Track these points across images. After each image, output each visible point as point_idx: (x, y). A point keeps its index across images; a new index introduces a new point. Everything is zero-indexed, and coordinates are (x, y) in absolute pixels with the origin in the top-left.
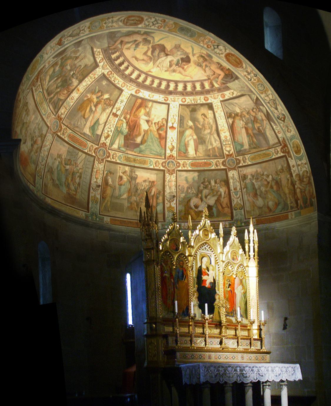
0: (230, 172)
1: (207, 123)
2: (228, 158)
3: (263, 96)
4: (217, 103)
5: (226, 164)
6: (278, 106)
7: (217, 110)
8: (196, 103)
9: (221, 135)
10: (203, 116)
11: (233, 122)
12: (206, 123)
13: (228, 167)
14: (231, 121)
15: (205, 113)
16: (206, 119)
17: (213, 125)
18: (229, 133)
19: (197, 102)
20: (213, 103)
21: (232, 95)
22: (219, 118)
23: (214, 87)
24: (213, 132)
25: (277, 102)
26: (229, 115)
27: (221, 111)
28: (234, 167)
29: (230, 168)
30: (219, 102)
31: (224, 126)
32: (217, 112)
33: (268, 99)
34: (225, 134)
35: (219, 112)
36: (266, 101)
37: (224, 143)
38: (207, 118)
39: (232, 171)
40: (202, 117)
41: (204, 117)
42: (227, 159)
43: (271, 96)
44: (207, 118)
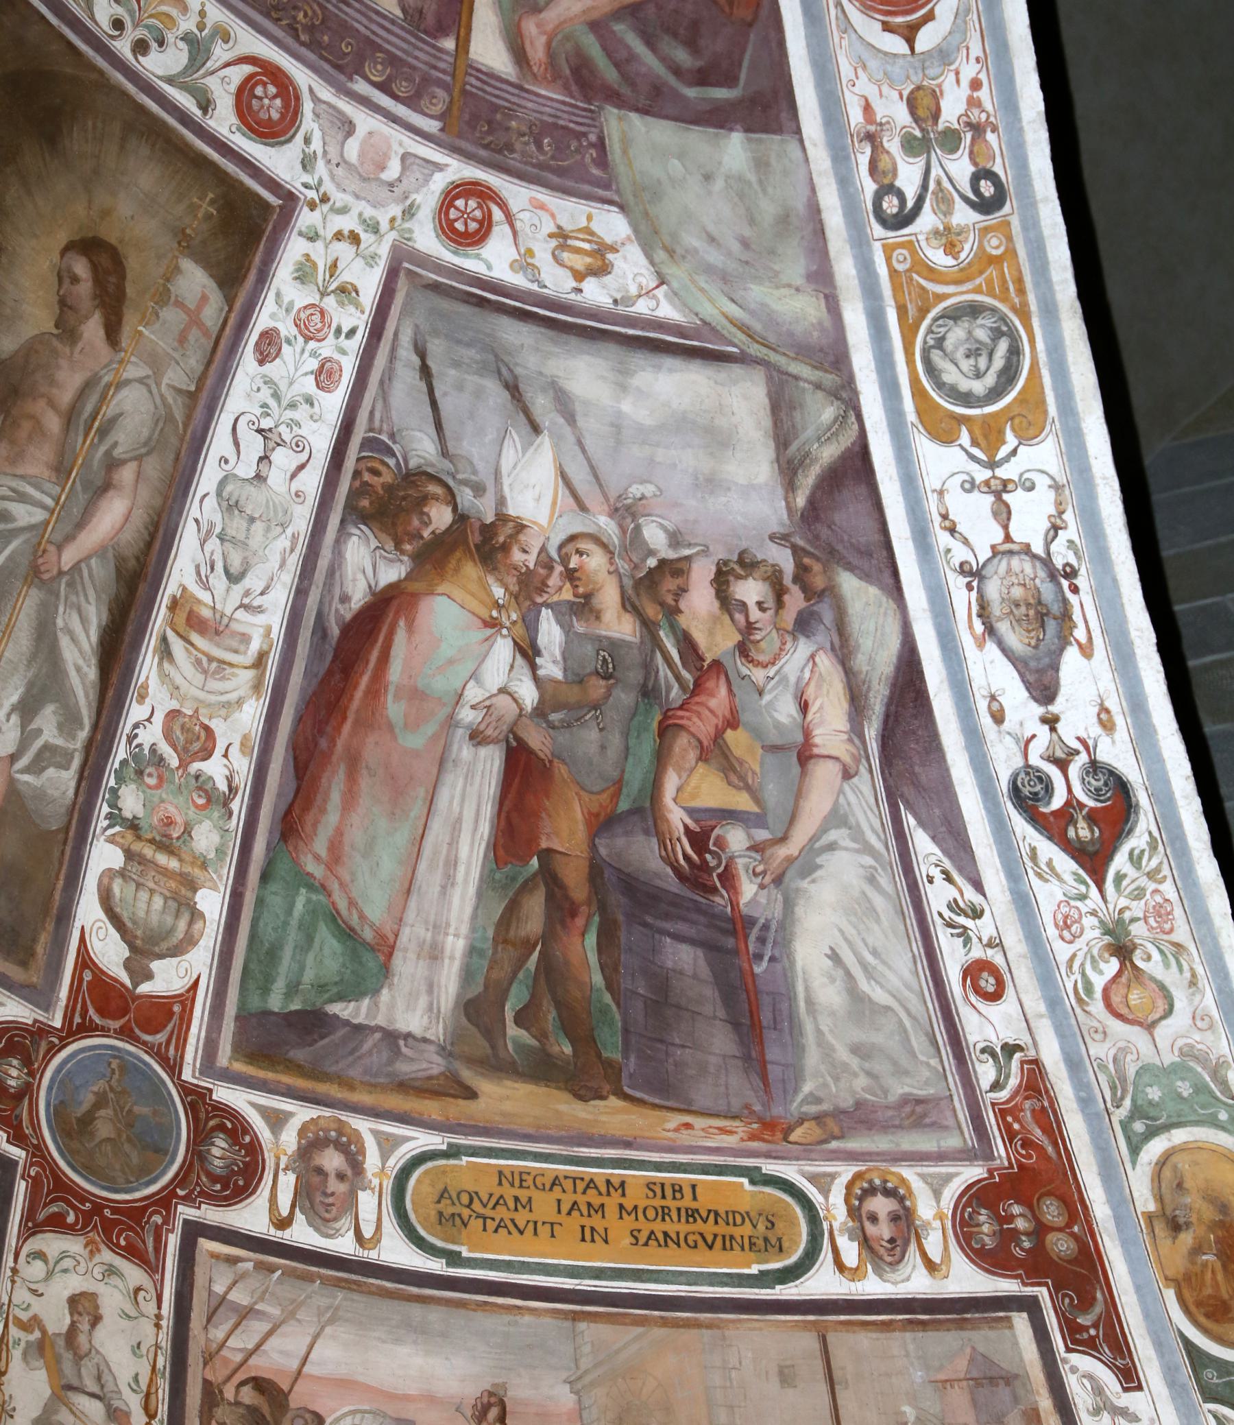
0: (52, 1243)
1: (66, 398)
2: (87, 1029)
3: (942, 463)
4: (344, 250)
5: (27, 1091)
6: (1071, 658)
7: (286, 328)
8: (123, 47)
9: (148, 667)
10: (81, 267)
11: (385, 608)
12: (69, 382)
13: (38, 1152)
14: (366, 565)
15: (133, 264)
16: (93, 329)
17: (126, 474)
18: (252, 715)
19: (141, 47)
20: (306, 218)
21: (579, 276)
22: (253, 446)
23: (449, 44)
24: (69, 557)
25: (1084, 605)
26: (377, 491)
27: (325, 375)
28: (135, 1214)
29: (62, 1188)
30: (371, 260)
31: (254, 581)
32: (269, 347)
33: (984, 534)
34: (211, 699)
35: (295, 366)
36: (944, 539)
37: (131, 802)
38: (112, 333)
39: (74, 1245)
40: (64, 277)
41: (85, 288)
42: (72, 1031)
43: (1030, 517)
44: (112, 333)
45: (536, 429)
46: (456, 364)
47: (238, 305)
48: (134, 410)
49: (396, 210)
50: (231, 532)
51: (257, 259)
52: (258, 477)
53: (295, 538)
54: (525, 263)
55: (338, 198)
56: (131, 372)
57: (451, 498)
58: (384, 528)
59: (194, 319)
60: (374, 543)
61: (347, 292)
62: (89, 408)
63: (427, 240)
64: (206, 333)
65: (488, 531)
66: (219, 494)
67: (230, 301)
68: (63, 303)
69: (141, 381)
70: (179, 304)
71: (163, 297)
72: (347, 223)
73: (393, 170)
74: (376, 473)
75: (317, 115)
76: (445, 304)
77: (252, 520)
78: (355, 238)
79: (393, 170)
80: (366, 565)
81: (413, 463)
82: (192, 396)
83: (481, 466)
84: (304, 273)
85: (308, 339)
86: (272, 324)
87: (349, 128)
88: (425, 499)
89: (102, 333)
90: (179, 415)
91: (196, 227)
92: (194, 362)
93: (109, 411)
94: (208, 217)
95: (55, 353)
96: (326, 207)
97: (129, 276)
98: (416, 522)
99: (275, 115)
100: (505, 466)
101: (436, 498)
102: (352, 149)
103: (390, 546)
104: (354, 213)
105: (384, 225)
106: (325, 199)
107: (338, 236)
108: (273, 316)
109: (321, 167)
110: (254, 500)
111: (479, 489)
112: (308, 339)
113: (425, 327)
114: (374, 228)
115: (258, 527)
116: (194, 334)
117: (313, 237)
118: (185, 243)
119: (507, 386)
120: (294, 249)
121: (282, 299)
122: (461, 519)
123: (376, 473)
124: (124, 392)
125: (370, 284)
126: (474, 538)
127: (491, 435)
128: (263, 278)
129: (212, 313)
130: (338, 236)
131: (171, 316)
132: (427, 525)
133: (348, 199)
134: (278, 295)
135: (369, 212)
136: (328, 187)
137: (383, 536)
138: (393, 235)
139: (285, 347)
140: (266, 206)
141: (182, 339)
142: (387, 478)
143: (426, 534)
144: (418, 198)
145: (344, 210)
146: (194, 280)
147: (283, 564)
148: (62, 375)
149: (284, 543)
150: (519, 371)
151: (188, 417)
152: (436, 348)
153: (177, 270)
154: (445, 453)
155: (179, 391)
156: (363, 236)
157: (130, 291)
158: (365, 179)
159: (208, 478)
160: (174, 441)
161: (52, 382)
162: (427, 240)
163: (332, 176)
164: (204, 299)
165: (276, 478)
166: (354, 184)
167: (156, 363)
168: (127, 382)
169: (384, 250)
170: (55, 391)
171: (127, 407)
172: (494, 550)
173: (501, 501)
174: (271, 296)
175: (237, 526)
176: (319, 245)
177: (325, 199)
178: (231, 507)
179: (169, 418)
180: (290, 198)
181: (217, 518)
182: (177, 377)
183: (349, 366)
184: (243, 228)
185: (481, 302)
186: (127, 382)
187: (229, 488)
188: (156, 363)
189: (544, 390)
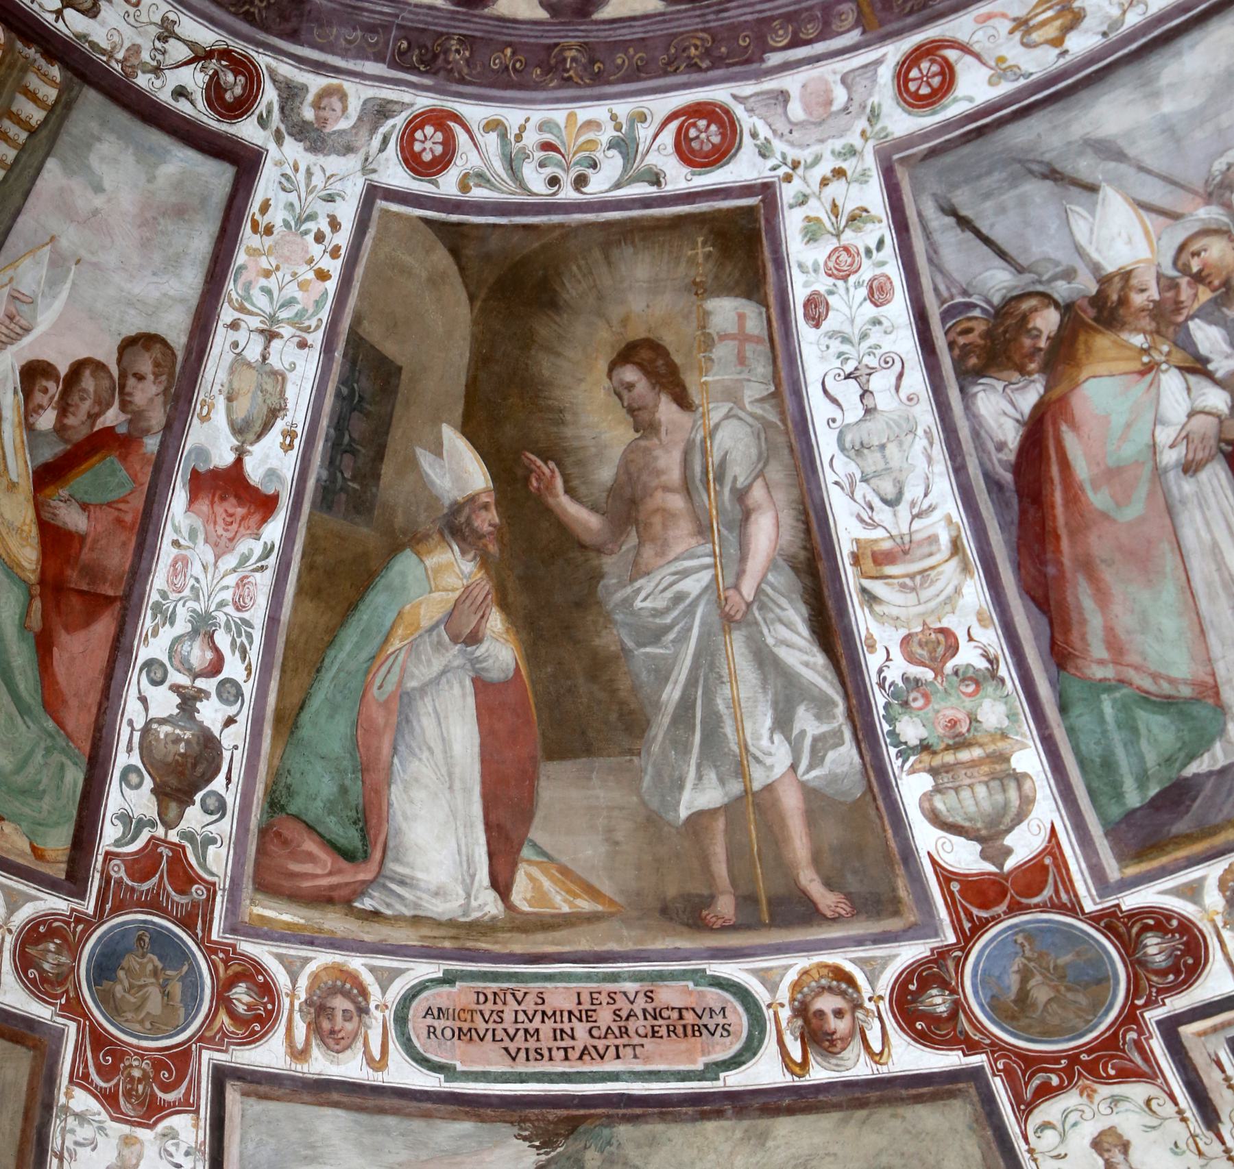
1: (675, 475)
7: (822, 284)
12: (670, 463)
14: (1001, 409)
15: (668, 339)
20: (788, 193)
44: (683, 401)
45: (1093, 189)
46: (987, 196)
47: (772, 300)
48: (734, 443)
49: (862, 123)
50: (870, 470)
51: (767, 254)
52: (868, 411)
53: (928, 433)
54: (1002, 70)
55: (805, 155)
56: (715, 417)
57: (1048, 299)
58: (1002, 367)
59: (743, 337)
60: (1000, 385)
61: (858, 218)
62: (698, 469)
63: (902, 123)
64: (758, 340)
65: (1098, 301)
66: (842, 448)
67: (764, 302)
68: (631, 411)
69: (727, 417)
70: (724, 337)
71: (708, 342)
72: (825, 168)
73: (840, 96)
74: (968, 331)
75: (750, 111)
76: (948, 159)
77: (882, 447)
78: (839, 173)
79: (840, 96)
80: (1001, 409)
81: (996, 300)
82: (776, 395)
83: (1059, 255)
84: (812, 233)
85: (845, 278)
86: (808, 291)
87: (783, 97)
88: (1025, 318)
89: (674, 407)
90: (773, 417)
91: (703, 271)
92: (762, 369)
93: (715, 458)
94: (708, 256)
95: (647, 451)
96: (800, 171)
97: (671, 349)
98: (1027, 342)
99: (716, 139)
100: (1082, 237)
101: (1034, 310)
102: (796, 110)
103: (1016, 376)
104: (827, 155)
105: (857, 142)
106: (795, 165)
107: (824, 182)
108: (806, 285)
109: (778, 146)
110: (875, 431)
111: (1069, 274)
112: (845, 278)
113: (939, 189)
114: (852, 152)
115: (892, 449)
116: (749, 348)
117: (803, 200)
118: (700, 290)
119: (1045, 177)
120: (792, 223)
121: (804, 262)
122: (1067, 309)
123: (968, 331)
124: (719, 436)
125: (873, 196)
126: (1089, 315)
127: (1053, 226)
128: (780, 263)
129: (754, 323)
130: (824, 182)
131: (723, 351)
132: (1038, 337)
133: (816, 149)
134: (800, 266)
135: (838, 144)
136: (793, 154)
137: (1005, 374)
138: (871, 143)
139: (831, 299)
140: (751, 210)
141: (742, 360)
142: (980, 327)
143: (1043, 344)
144: (875, 99)
145: (817, 160)
146: (726, 311)
147: (930, 460)
148: (662, 463)
149: (921, 442)
150: (1047, 157)
151: (782, 413)
152: (963, 199)
153: (707, 314)
154: (1020, 270)
155: (762, 400)
156: (844, 165)
157: (678, 359)
158: (820, 123)
159: (826, 443)
160: (781, 439)
161: (658, 473)
162: (902, 123)
163: (792, 144)
164: (741, 317)
165: (884, 400)
166: (815, 133)
167: (732, 395)
168: (717, 426)
169: (870, 161)
170: (664, 478)
171: (728, 444)
172: (1113, 311)
173: (1096, 268)
174: (795, 271)
175: (873, 461)
176: (813, 202)
177: (795, 165)
178: (858, 451)
179: (767, 425)
180: (767, 190)
181: (853, 468)
182: (755, 390)
183: (894, 271)
184: (741, 243)
185: (980, 132)
186: (717, 426)
187: (848, 439)
188: (732, 395)
189: (1081, 154)
